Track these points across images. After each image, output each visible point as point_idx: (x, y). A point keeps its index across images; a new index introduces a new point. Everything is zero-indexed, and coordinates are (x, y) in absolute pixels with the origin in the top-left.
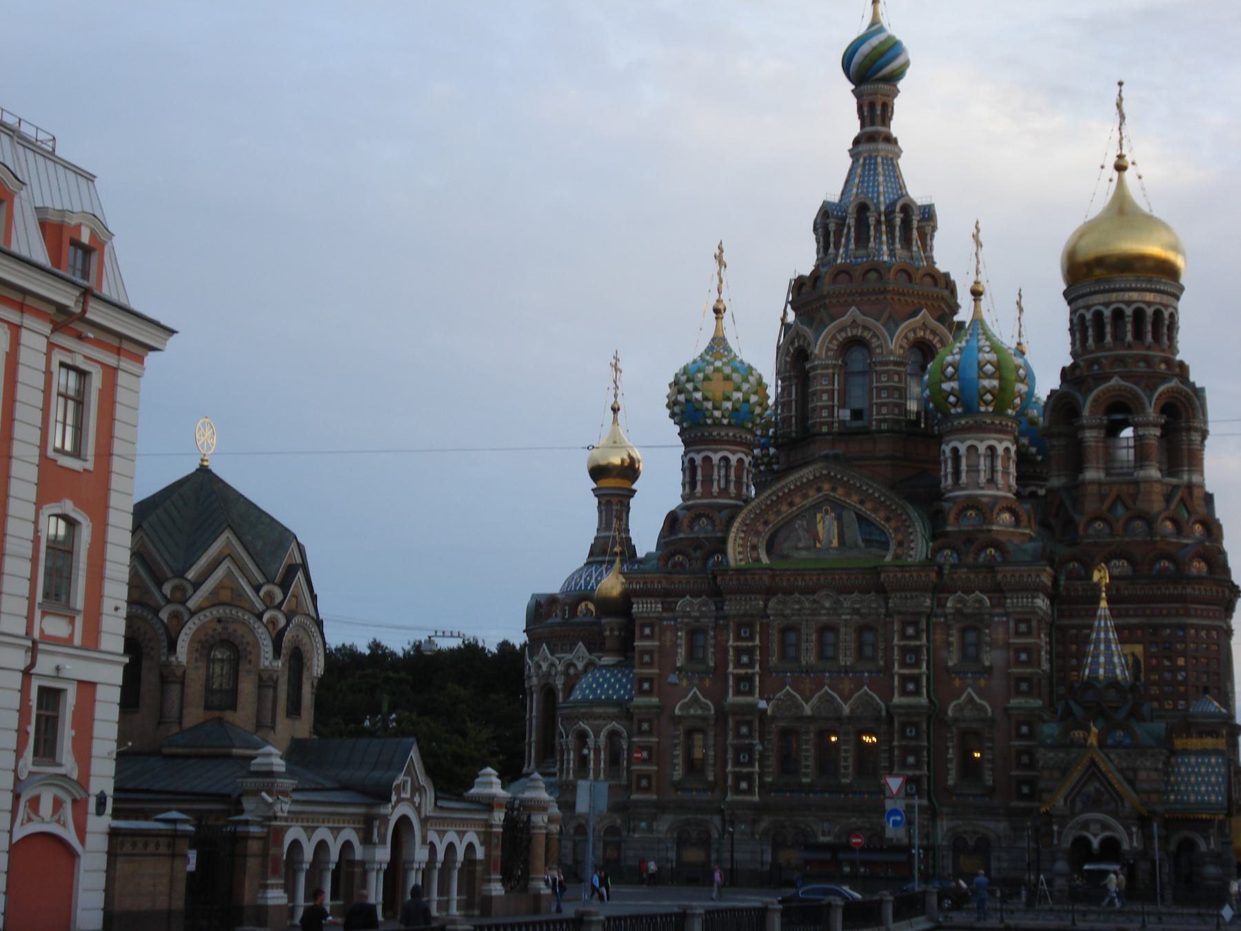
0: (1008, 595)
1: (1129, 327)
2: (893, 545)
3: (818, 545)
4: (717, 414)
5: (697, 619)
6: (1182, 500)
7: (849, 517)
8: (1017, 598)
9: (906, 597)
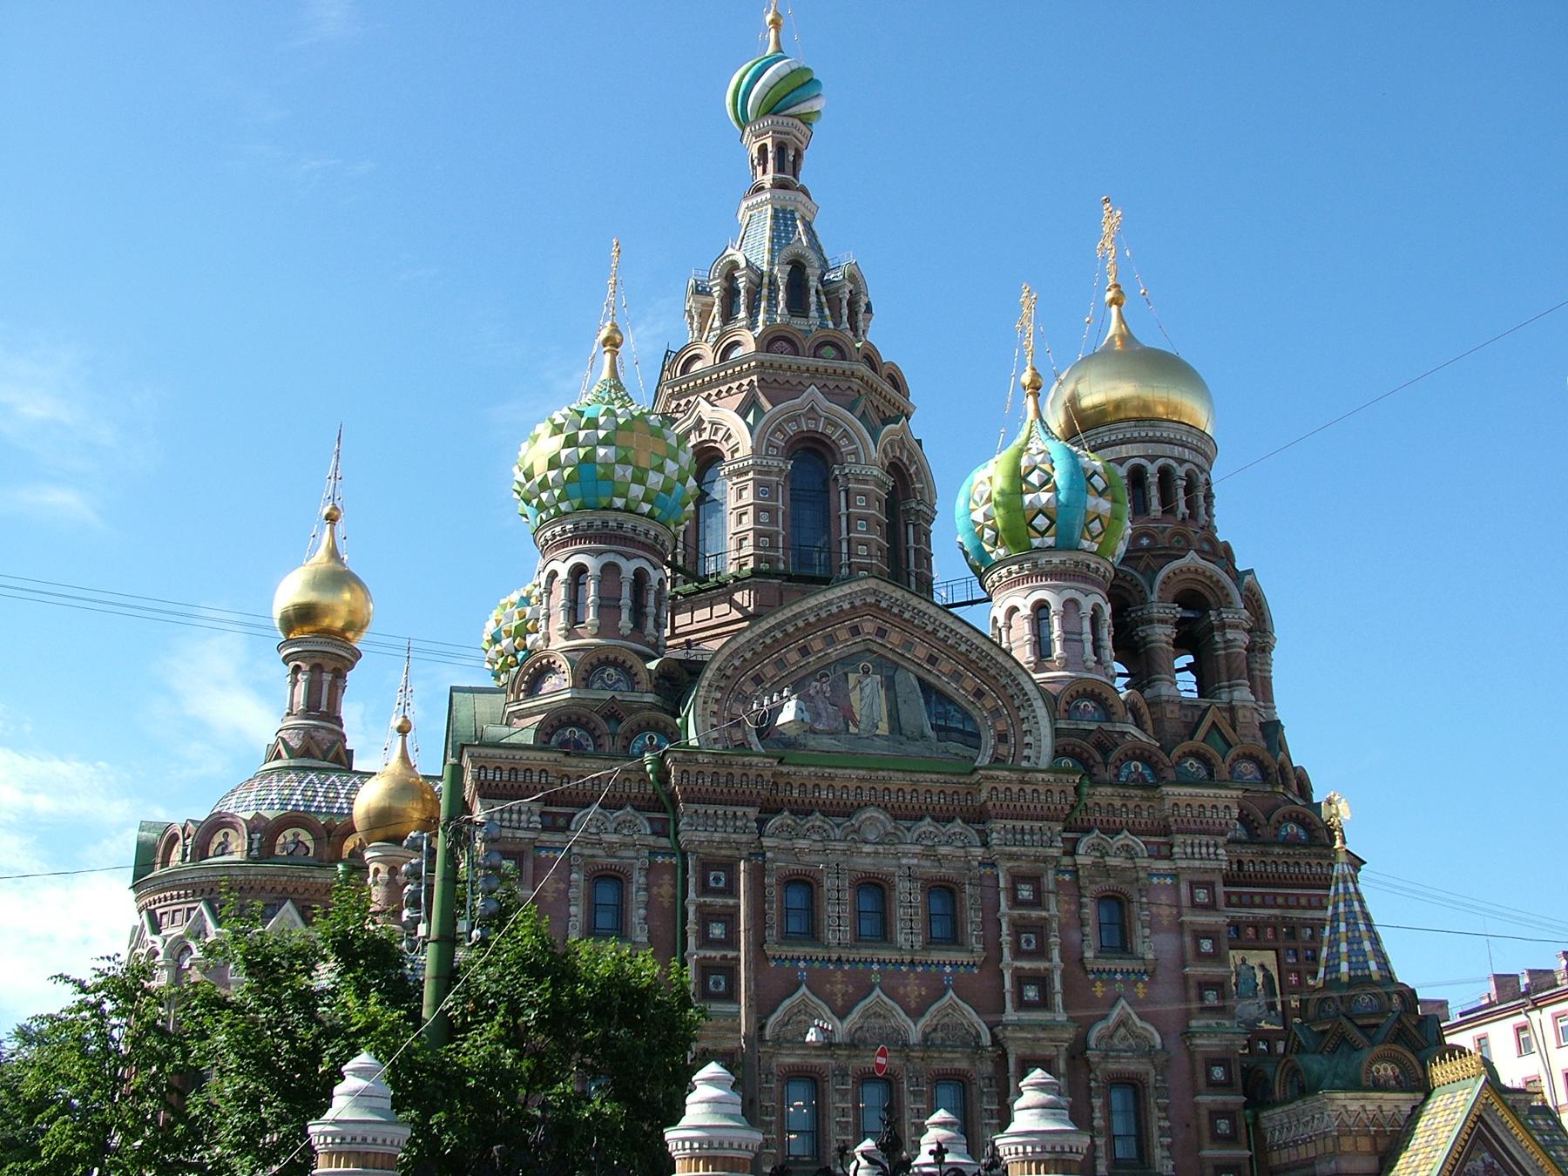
0: (1179, 839)
1: (1181, 493)
2: (989, 739)
3: (852, 729)
7: (907, 683)
8: (1192, 845)
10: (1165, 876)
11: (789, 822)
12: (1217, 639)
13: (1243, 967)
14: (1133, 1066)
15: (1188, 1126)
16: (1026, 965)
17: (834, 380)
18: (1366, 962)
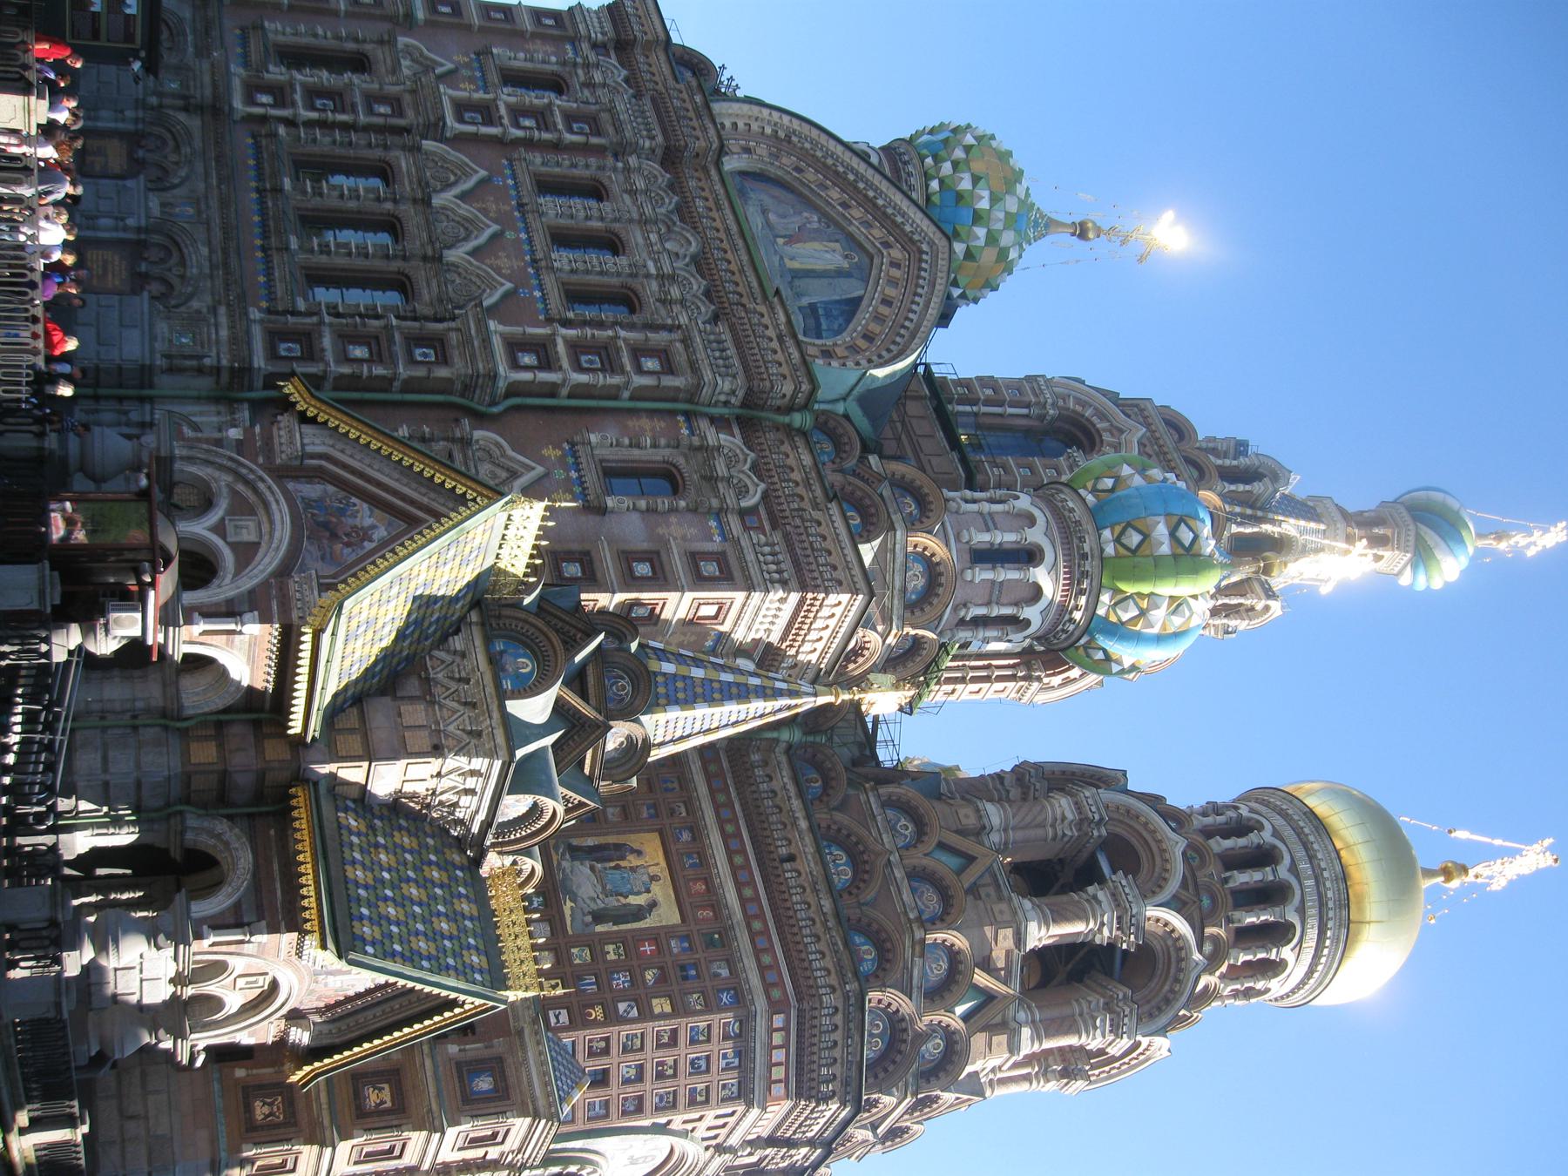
0: (777, 537)
3: (780, 241)
4: (947, 168)
5: (589, 84)
7: (852, 289)
9: (723, 350)
10: (722, 534)
11: (660, 180)
12: (1090, 889)
13: (645, 878)
16: (561, 348)
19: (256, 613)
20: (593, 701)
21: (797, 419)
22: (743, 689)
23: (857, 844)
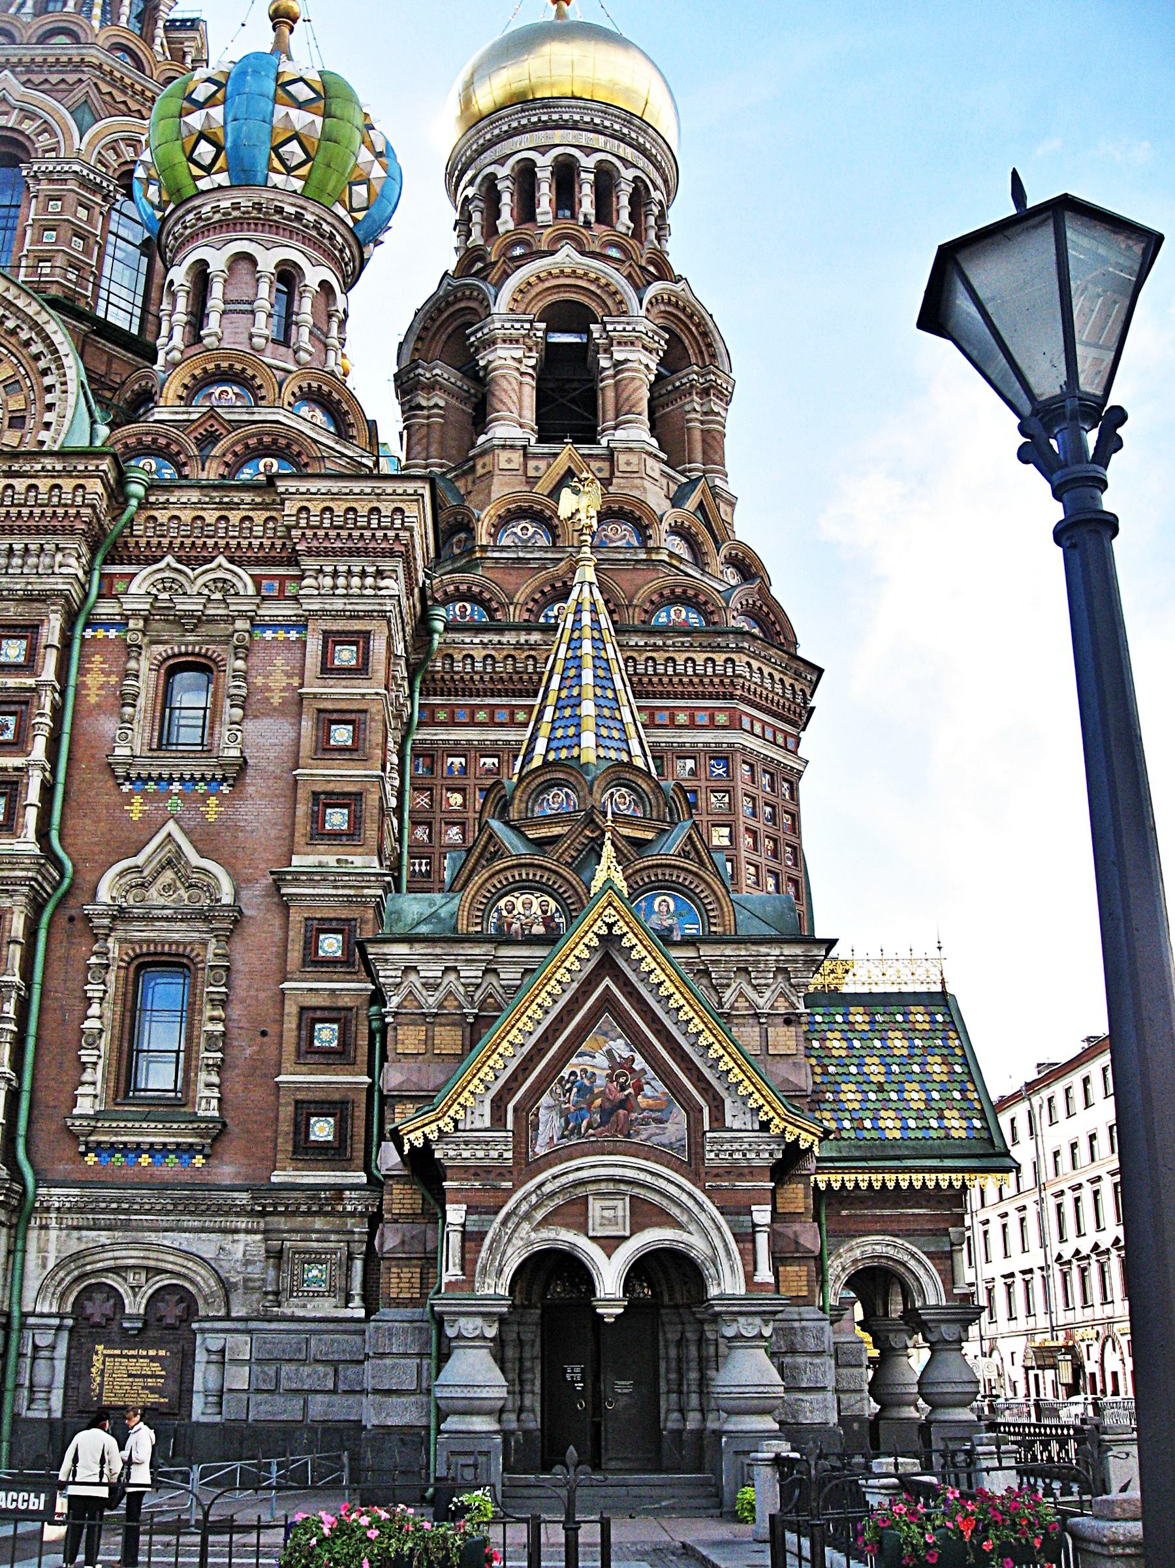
0: (309, 563)
1: (587, 189)
6: (701, 506)
8: (335, 574)
10: (288, 628)
12: (604, 363)
14: (179, 933)
15: (264, 1034)
17: (59, 72)
18: (579, 735)
19: (753, 1208)
20: (650, 836)
21: (137, 489)
22: (598, 663)
23: (553, 586)
